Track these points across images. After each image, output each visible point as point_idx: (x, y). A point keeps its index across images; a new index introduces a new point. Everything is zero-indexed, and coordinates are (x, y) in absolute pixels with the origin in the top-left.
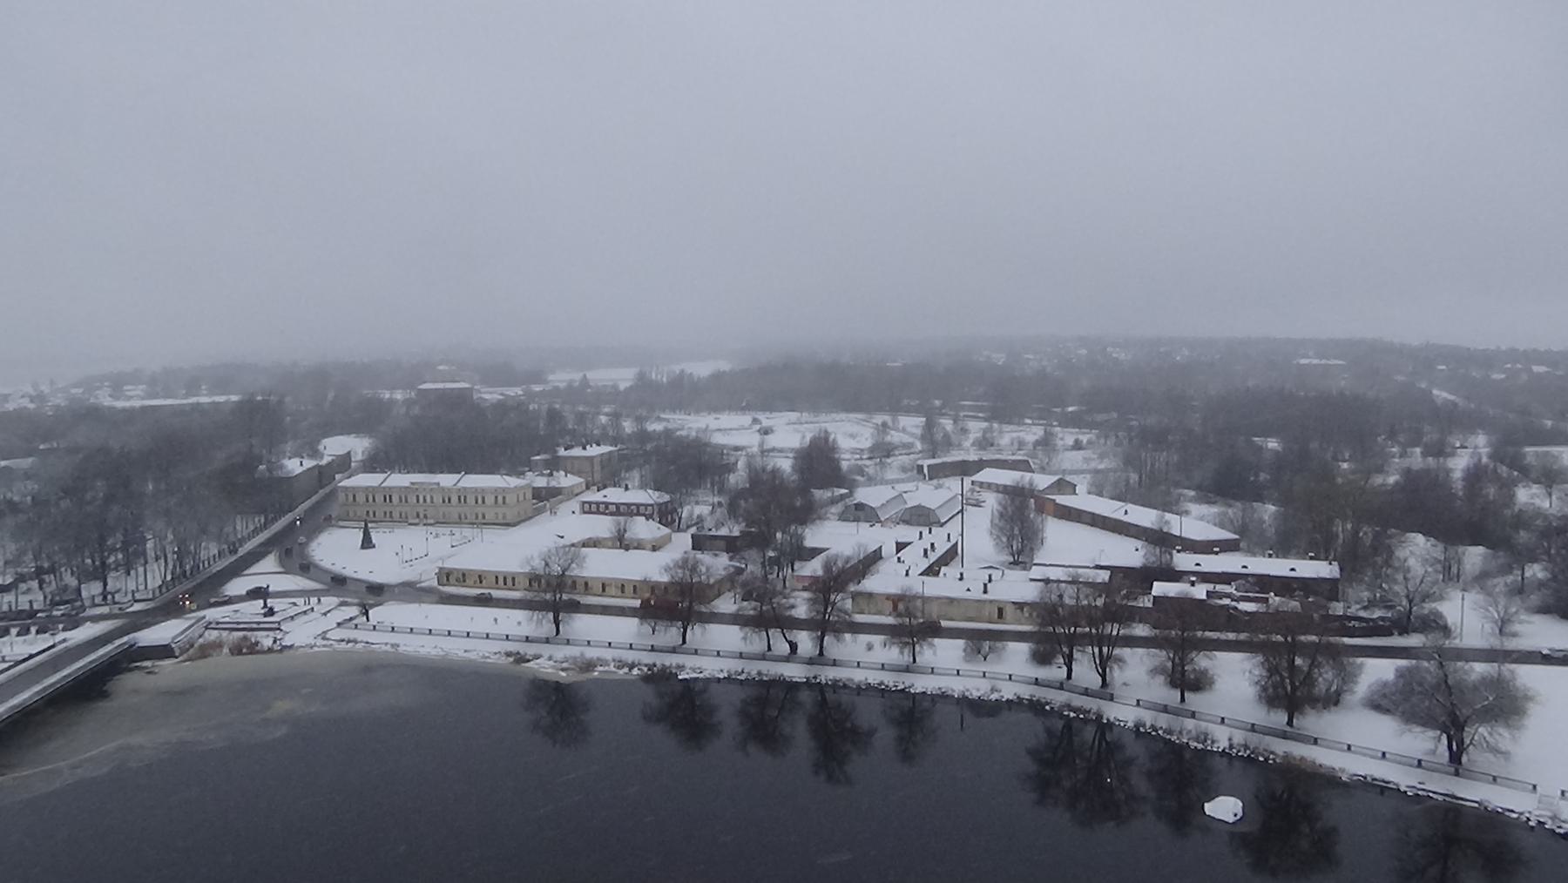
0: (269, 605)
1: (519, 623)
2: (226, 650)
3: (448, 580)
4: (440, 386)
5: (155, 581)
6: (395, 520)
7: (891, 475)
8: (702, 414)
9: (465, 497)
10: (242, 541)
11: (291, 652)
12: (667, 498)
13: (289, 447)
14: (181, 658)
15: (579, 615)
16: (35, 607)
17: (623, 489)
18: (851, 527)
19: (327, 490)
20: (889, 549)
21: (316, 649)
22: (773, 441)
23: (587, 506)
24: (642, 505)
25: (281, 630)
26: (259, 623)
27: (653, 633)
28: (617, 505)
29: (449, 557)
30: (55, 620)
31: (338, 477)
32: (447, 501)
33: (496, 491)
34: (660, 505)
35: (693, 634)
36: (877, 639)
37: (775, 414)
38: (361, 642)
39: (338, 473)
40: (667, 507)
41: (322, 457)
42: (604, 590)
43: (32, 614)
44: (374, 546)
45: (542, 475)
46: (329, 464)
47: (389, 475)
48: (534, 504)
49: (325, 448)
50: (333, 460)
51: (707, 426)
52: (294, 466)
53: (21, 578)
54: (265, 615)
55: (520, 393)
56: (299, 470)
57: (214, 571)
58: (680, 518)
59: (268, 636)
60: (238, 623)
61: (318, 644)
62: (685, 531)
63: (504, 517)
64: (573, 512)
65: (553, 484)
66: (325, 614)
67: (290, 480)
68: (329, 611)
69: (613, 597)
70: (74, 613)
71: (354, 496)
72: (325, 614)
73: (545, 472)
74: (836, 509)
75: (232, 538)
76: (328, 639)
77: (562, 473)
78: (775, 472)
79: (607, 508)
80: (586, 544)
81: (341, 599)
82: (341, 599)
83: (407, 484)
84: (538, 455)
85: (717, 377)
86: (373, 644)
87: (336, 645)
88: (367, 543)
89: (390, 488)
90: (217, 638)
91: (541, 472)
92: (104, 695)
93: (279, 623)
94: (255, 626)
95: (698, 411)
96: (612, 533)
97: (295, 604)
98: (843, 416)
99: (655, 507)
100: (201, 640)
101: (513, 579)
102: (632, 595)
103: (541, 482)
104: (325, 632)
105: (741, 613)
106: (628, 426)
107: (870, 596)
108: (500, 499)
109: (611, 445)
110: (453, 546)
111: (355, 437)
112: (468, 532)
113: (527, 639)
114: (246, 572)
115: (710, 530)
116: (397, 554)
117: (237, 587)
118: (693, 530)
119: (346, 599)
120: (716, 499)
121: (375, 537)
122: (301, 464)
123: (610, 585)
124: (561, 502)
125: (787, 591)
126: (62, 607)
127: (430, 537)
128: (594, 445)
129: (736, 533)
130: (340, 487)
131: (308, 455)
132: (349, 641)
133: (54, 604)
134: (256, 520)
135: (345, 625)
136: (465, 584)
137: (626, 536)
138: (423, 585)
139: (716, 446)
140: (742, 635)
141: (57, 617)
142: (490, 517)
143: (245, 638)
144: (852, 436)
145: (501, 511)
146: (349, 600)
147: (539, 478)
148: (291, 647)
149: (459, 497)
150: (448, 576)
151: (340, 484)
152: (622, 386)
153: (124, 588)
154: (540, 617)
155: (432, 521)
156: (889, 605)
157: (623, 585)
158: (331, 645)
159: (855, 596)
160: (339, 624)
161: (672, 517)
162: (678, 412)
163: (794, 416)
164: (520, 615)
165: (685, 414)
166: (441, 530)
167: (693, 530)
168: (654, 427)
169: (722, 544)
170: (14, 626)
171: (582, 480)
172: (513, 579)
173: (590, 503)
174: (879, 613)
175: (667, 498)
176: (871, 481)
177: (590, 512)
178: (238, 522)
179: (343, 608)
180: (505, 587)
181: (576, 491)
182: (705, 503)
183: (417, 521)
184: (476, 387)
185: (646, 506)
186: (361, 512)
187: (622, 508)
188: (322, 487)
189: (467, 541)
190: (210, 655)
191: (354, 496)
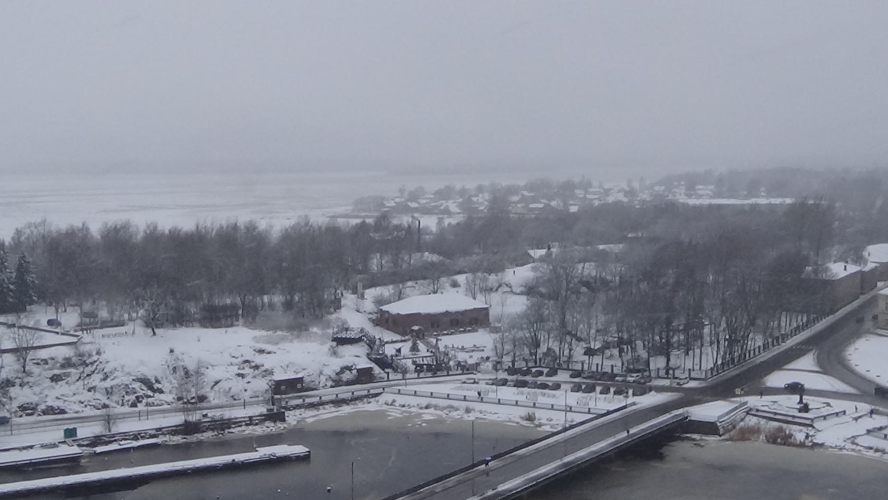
0: (804, 401)
2: (762, 437)
5: (708, 363)
10: (785, 337)
11: (822, 450)
13: (835, 251)
14: (722, 438)
16: (616, 371)
25: (814, 427)
26: (794, 417)
30: (628, 385)
31: (880, 284)
41: (866, 264)
43: (612, 376)
46: (872, 271)
49: (869, 255)
50: (876, 267)
52: (839, 270)
53: (607, 346)
54: (800, 411)
56: (842, 274)
57: (758, 361)
59: (801, 431)
60: (775, 414)
61: (846, 447)
66: (856, 419)
67: (830, 284)
68: (860, 417)
70: (643, 381)
72: (856, 419)
75: (777, 334)
76: (857, 445)
82: (873, 407)
87: (864, 452)
90: (756, 424)
92: (661, 457)
93: (812, 420)
94: (790, 419)
97: (828, 405)
100: (742, 424)
114: (786, 367)
117: (777, 379)
119: (877, 408)
122: (845, 269)
126: (635, 375)
131: (853, 260)
132: (877, 450)
133: (630, 371)
134: (800, 318)
135: (872, 433)
141: (629, 382)
143: (780, 429)
146: (881, 409)
148: (822, 445)
151: (882, 292)
153: (683, 366)
158: (859, 450)
170: (600, 385)
178: (783, 319)
190: (749, 439)
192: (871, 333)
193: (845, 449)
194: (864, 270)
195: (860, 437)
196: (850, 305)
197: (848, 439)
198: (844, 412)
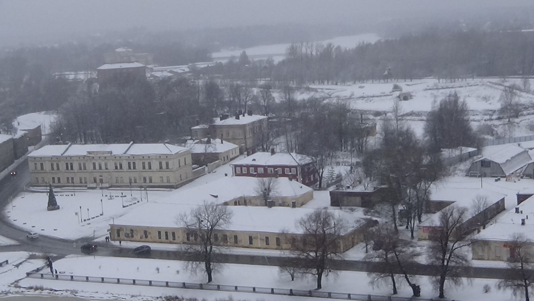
1: (178, 272)
3: (119, 236)
4: (117, 66)
6: (75, 185)
7: (518, 133)
8: (348, 83)
9: (134, 163)
12: (307, 160)
15: (227, 264)
17: (270, 153)
18: (475, 182)
19: (21, 160)
20: (511, 201)
21: (10, 295)
22: (406, 107)
23: (238, 169)
24: (287, 167)
27: (293, 280)
28: (265, 168)
29: (120, 216)
31: (30, 148)
32: (119, 168)
33: (160, 157)
34: (303, 167)
35: (327, 280)
36: (492, 282)
37: (415, 81)
38: (46, 289)
39: (30, 146)
40: (309, 169)
41: (15, 131)
42: (251, 243)
44: (58, 208)
45: (201, 142)
46: (22, 137)
47: (70, 146)
48: (194, 169)
49: (19, 124)
50: (25, 134)
51: (353, 94)
55: (187, 70)
58: (321, 178)
62: (325, 189)
63: (168, 181)
64: (226, 175)
65: (210, 150)
66: (17, 266)
68: (21, 263)
69: (259, 248)
71: (42, 164)
72: (17, 266)
73: (202, 140)
74: (464, 166)
76: (20, 287)
77: (218, 140)
78: (408, 135)
79: (256, 171)
80: (237, 202)
81: (31, 253)
82: (31, 253)
83: (85, 154)
84: (198, 125)
85: (363, 49)
86: (58, 291)
87: (26, 292)
88: (53, 205)
89: (71, 157)
91: (200, 140)
95: (344, 81)
96: (258, 192)
98: (477, 80)
99: (298, 169)
101: (174, 234)
102: (276, 246)
103: (199, 149)
104: (17, 281)
105: (367, 260)
106: (277, 97)
107: (485, 243)
108: (164, 166)
109: (263, 115)
110: (124, 207)
111: (45, 114)
112: (137, 194)
113: (184, 286)
115: (348, 187)
116: (76, 214)
118: (332, 189)
119: (34, 253)
120: (354, 160)
121: (59, 199)
123: (256, 238)
124: (218, 166)
125: (415, 241)
127: (105, 199)
128: (246, 115)
129: (370, 190)
130: (31, 157)
131: (4, 130)
132: (37, 289)
136: (133, 239)
137: (271, 194)
138: (95, 240)
139: (354, 112)
140: (369, 279)
142: (156, 180)
144: (485, 99)
145: (165, 175)
147: (200, 145)
149: (129, 164)
150: (118, 231)
152: (277, 60)
154: (194, 266)
155: (107, 185)
156: (505, 253)
157: (267, 238)
159: (474, 243)
160: (28, 274)
161: (314, 176)
162: (326, 82)
163: (431, 82)
164: (176, 265)
165: (332, 84)
166: (114, 193)
167: (332, 189)
168: (300, 97)
169: (358, 200)
171: (237, 146)
172: (174, 234)
173: (241, 166)
174: (499, 259)
175: (307, 160)
176: (500, 139)
177: (242, 175)
179: (32, 261)
180: (167, 241)
181: (231, 156)
182: (344, 163)
183: (94, 185)
184: (149, 66)
185: (290, 167)
186: (48, 178)
187: (269, 170)
188: (16, 157)
189: (136, 201)
191: (42, 164)
192: (24, 191)
193: (10, 293)
194: (15, 138)
195: (22, 280)
196: (7, 169)
197: (12, 284)
198: (7, 261)
